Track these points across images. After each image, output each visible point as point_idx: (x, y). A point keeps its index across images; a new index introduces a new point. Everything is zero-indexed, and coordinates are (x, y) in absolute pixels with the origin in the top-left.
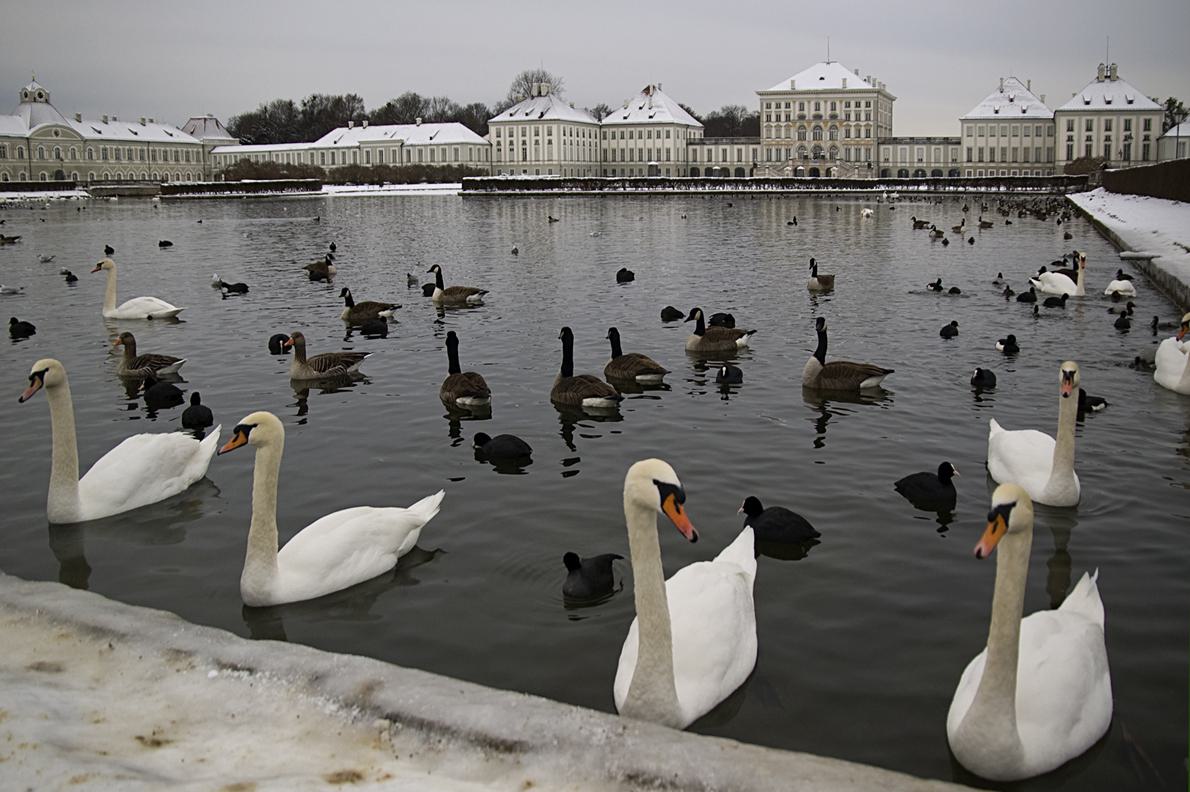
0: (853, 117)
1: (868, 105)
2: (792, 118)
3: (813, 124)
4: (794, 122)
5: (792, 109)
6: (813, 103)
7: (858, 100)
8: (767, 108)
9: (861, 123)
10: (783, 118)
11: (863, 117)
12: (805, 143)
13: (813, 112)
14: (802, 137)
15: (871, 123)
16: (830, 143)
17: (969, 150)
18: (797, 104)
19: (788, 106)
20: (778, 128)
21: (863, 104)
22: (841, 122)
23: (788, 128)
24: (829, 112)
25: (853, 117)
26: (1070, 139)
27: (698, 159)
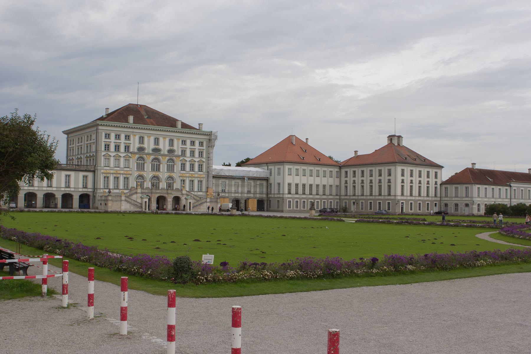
0: (188, 153)
1: (201, 144)
2: (131, 150)
3: (152, 157)
5: (132, 141)
6: (152, 139)
7: (193, 140)
9: (194, 159)
10: (122, 149)
11: (197, 154)
12: (145, 174)
13: (152, 146)
14: (141, 167)
15: (204, 160)
16: (167, 175)
17: (289, 185)
19: (127, 137)
20: (117, 158)
21: (197, 143)
22: (178, 156)
23: (127, 159)
24: (167, 148)
25: (188, 153)
26: (403, 181)
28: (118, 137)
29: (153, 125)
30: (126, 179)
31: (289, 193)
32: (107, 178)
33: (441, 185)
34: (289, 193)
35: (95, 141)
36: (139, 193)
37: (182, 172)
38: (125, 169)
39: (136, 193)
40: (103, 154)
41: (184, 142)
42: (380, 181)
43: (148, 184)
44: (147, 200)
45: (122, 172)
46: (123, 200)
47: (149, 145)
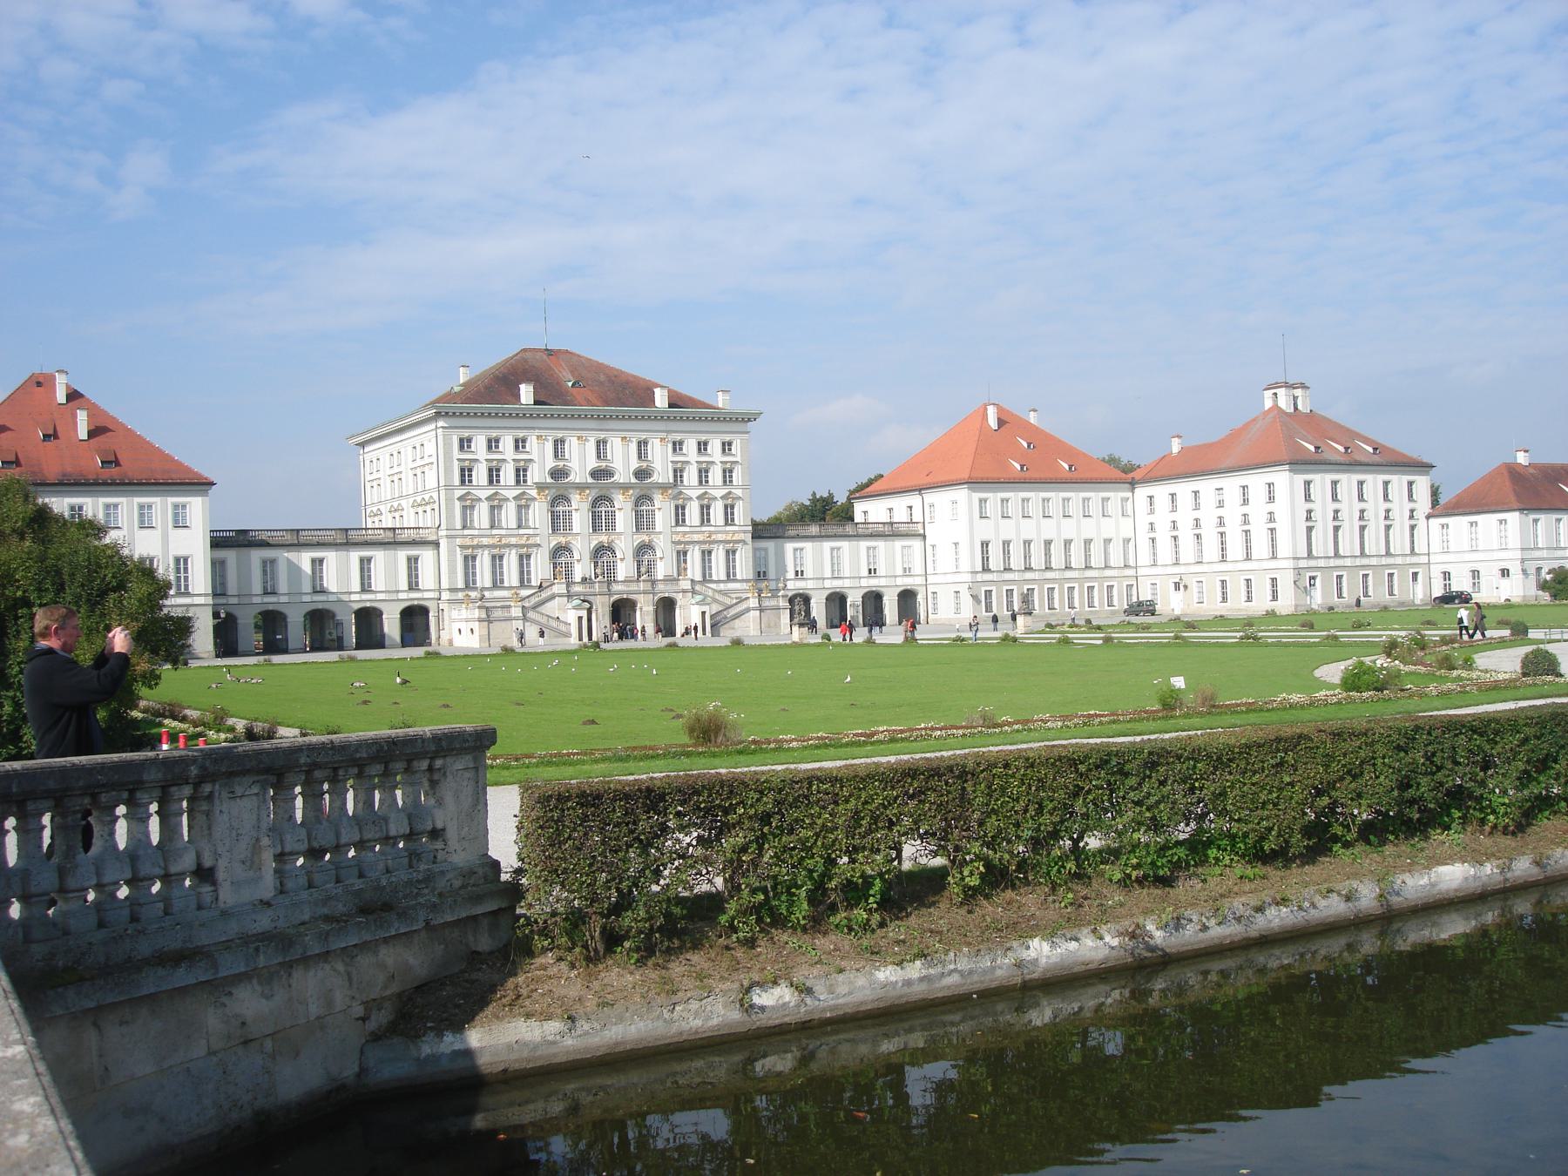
0: (691, 476)
1: (726, 447)
3: (591, 494)
4: (541, 487)
6: (591, 447)
8: (461, 448)
10: (508, 475)
11: (716, 475)
13: (592, 463)
14: (558, 522)
15: (739, 492)
18: (549, 446)
19: (519, 444)
24: (635, 464)
25: (691, 476)
27: (232, 588)
28: (493, 444)
29: (589, 403)
30: (524, 559)
31: (986, 569)
32: (469, 560)
33: (1428, 517)
34: (986, 569)
35: (434, 459)
36: (560, 596)
37: (679, 529)
38: (521, 531)
39: (553, 597)
40: (459, 493)
41: (677, 446)
42: (1246, 519)
43: (582, 568)
44: (584, 614)
45: (513, 541)
46: (516, 619)
47: (581, 459)
